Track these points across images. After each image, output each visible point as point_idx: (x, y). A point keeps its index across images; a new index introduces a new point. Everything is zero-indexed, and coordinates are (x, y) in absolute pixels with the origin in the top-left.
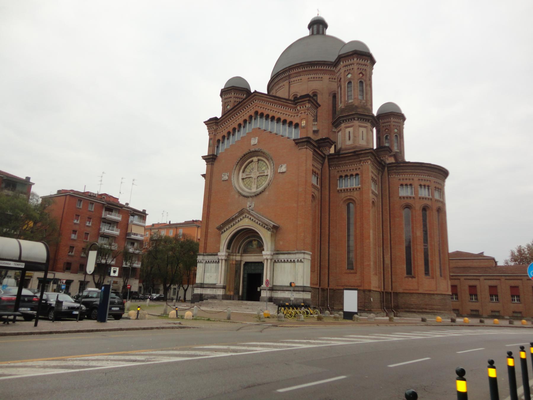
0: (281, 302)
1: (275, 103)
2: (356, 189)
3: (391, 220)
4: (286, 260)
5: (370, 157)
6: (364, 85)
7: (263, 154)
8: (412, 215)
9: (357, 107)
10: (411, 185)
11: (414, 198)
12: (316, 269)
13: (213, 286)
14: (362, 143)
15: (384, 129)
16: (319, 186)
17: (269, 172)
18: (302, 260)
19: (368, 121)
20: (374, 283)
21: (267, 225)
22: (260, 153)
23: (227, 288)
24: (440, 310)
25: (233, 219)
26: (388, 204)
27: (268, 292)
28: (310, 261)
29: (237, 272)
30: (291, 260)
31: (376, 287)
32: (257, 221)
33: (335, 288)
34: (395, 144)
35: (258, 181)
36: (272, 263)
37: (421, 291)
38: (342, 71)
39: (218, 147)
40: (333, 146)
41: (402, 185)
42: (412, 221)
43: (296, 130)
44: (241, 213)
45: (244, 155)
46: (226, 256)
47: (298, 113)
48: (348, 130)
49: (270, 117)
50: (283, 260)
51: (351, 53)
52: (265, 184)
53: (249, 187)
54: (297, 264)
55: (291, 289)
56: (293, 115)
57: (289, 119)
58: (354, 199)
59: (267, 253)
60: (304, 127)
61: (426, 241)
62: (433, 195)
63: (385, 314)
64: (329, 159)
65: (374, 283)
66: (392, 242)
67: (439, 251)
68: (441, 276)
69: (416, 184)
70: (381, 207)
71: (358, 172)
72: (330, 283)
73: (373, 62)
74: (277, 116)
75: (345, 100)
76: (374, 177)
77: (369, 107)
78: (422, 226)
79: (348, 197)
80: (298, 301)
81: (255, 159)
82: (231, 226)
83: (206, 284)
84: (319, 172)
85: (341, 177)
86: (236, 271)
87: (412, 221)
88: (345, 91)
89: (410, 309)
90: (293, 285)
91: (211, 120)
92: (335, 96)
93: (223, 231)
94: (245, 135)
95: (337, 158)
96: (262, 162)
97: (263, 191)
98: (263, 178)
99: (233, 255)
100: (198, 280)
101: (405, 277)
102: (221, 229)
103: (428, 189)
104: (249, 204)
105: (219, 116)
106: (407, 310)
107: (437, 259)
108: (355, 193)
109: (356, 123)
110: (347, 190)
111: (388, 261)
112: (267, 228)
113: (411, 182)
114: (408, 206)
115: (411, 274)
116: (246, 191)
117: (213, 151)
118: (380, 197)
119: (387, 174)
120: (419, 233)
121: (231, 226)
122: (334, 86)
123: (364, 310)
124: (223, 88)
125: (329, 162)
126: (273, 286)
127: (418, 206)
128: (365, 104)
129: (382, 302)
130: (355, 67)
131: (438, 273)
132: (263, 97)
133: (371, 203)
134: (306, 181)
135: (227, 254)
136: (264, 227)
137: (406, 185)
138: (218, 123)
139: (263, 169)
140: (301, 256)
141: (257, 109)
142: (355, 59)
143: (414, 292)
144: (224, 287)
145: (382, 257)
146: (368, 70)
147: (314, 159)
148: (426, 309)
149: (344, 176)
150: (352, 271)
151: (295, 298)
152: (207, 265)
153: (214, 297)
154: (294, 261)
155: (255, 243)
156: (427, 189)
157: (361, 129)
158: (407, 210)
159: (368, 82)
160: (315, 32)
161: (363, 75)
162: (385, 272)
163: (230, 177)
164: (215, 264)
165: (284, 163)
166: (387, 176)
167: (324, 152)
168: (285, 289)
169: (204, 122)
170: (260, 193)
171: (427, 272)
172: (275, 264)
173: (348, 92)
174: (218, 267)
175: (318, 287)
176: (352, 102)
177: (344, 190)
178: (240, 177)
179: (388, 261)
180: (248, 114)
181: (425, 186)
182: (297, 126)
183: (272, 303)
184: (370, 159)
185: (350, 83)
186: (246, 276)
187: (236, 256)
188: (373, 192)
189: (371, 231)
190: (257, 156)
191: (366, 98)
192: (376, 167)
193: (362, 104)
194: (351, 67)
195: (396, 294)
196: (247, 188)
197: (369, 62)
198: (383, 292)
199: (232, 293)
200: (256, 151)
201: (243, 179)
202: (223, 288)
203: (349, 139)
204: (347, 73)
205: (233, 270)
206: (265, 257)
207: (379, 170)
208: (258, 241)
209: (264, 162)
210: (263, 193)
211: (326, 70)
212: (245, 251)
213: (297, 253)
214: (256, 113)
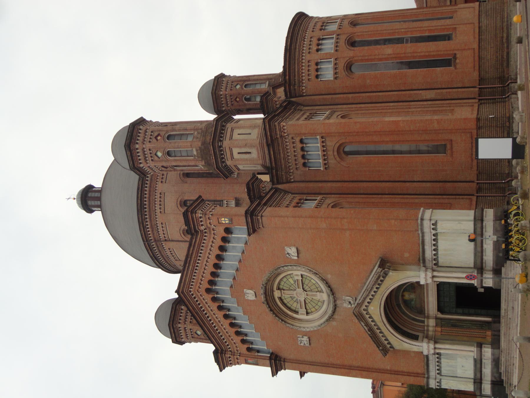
0: (501, 255)
1: (195, 262)
2: (323, 142)
3: (370, 90)
4: (434, 248)
5: (276, 124)
6: (172, 133)
7: (270, 281)
8: (362, 60)
9: (203, 143)
10: (317, 64)
11: (336, 59)
12: (446, 201)
13: (478, 364)
14: (255, 134)
15: (236, 103)
16: (319, 198)
17: (297, 273)
18: (433, 222)
19: (224, 126)
20: (466, 113)
21: (379, 277)
22: (268, 287)
23: (480, 340)
24: (502, 18)
25: (370, 329)
26: (345, 95)
27: (485, 275)
28: (434, 211)
29: (455, 324)
30: (434, 240)
31: (473, 110)
32: (373, 293)
33: (476, 172)
34: (258, 87)
35: (311, 291)
36: (439, 269)
37: (476, 46)
38: (152, 164)
39: (258, 351)
40: (259, 176)
41: (317, 77)
42: (372, 60)
43: (234, 231)
44: (360, 317)
45: (271, 310)
46: (429, 343)
47: (209, 228)
48: (236, 156)
49: (214, 270)
50: (434, 252)
51: (129, 153)
52: (315, 280)
53: (319, 304)
54: (439, 230)
55: (479, 239)
56: (213, 235)
57: (219, 242)
58: (338, 145)
59: (422, 277)
60: (231, 220)
61: (400, 41)
62: (332, 33)
63: (513, 96)
64: (278, 183)
65: (466, 113)
66: (403, 89)
67: (413, 21)
68: (452, 18)
69: (315, 57)
70: (349, 106)
71: (298, 139)
72: (468, 180)
73: (141, 121)
74: (213, 260)
75: (193, 160)
76: (305, 116)
77: (204, 125)
78: (378, 46)
79: (336, 153)
80: (499, 229)
81: (277, 294)
82: (381, 332)
83: (475, 374)
84: (298, 197)
85: (304, 165)
86: (454, 326)
87: (372, 60)
88: (180, 160)
89: (505, 60)
90: (472, 237)
91: (217, 360)
92: (187, 175)
93: (388, 346)
94: (240, 309)
95: (277, 171)
96: (282, 283)
97: (327, 283)
98: (306, 282)
99: (428, 330)
100: (470, 387)
101: (455, 66)
102: (385, 349)
103: (323, 39)
104: (346, 305)
105: (211, 348)
106: (505, 64)
107: (426, 24)
108: (328, 143)
109: (226, 143)
110: (324, 155)
111: (431, 94)
112: (384, 277)
113: (313, 64)
114: (349, 67)
115: (450, 60)
116: (326, 308)
117: (264, 358)
118: (336, 107)
119: (301, 98)
120: (388, 50)
121: (381, 332)
122: (173, 176)
123: (509, 127)
124: (171, 340)
125: (283, 183)
126: (475, 267)
127: (348, 53)
128: (200, 131)
129: (494, 101)
130: (148, 146)
131: (448, 22)
132: (185, 280)
133: (343, 121)
134: (311, 217)
135: (425, 340)
136: (382, 281)
137: (317, 70)
138: (222, 350)
139: (292, 282)
140: (427, 225)
141: (202, 291)
142: (137, 146)
143: (477, 55)
144: (480, 346)
145: (425, 103)
146: (152, 128)
147: (278, 205)
148: (502, 37)
149: (303, 161)
150: (448, 146)
151: (494, 234)
152: (444, 372)
153: (496, 362)
154: (434, 235)
155: (407, 296)
156: (324, 42)
157: (235, 136)
158: (353, 69)
159: (169, 128)
160: (98, 203)
161: (159, 135)
162: (449, 97)
163: (305, 334)
164: (442, 360)
165: (284, 250)
166: (304, 98)
167: (268, 190)
168: (479, 249)
169: (221, 371)
170: (329, 287)
171: (448, 38)
172: (440, 264)
173: (181, 156)
174: (447, 354)
175: (474, 198)
176: (197, 150)
177: (325, 160)
178: (305, 317)
179: (431, 94)
180: (210, 303)
181: (318, 45)
182: (228, 231)
183: (503, 270)
184: (279, 123)
185: (169, 154)
186: (460, 311)
187: (428, 326)
188: (328, 118)
189: (387, 119)
190: (273, 291)
191: (191, 130)
192: (290, 115)
193: (199, 136)
194: (147, 152)
195: (481, 80)
196: (321, 307)
197: (141, 127)
198: (479, 100)
199: (489, 333)
200: (265, 293)
201: (307, 313)
202: (481, 347)
203: (250, 153)
204: (156, 158)
205: (450, 332)
206: (430, 281)
207: (295, 109)
208: (404, 291)
209: (281, 280)
210: (329, 281)
211: (150, 187)
212: (421, 311)
213: (422, 230)
214: (208, 291)
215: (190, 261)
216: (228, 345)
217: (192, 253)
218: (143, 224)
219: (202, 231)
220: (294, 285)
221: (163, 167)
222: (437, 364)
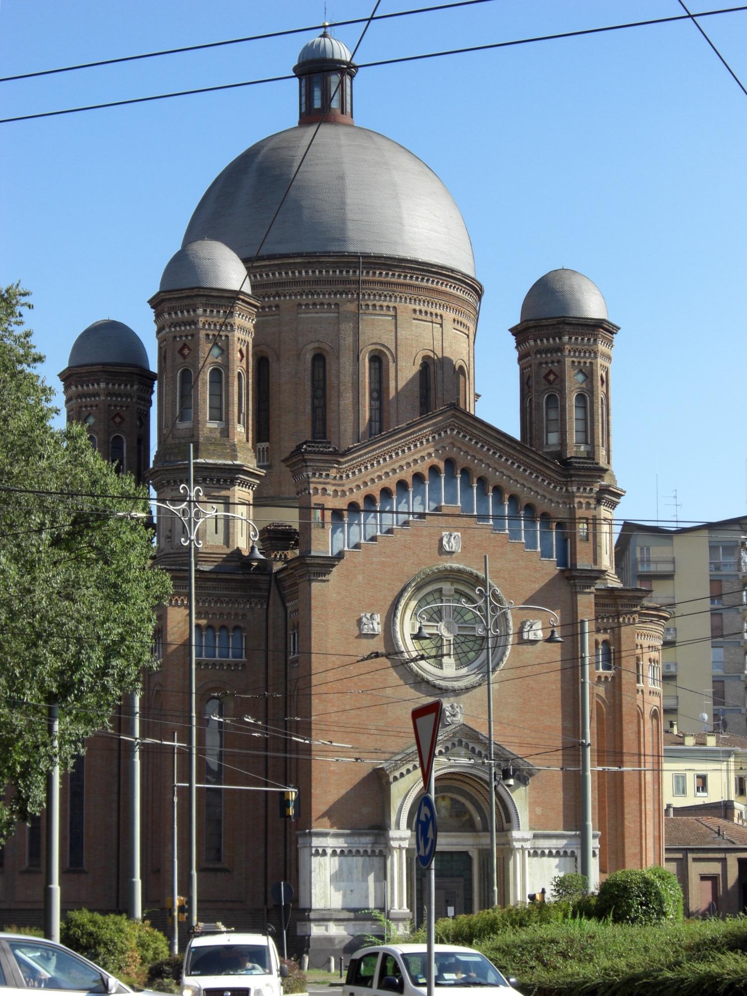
4: (554, 851)
50: (547, 851)
59: (521, 834)
93: (397, 774)
132: (475, 427)
154: (573, 852)
164: (360, 858)
208: (452, 799)
215: (514, 449)
216: (348, 476)
217: (528, 456)
218: (396, 266)
219: (566, 485)
220: (462, 620)
221: (551, 372)
222: (354, 850)
